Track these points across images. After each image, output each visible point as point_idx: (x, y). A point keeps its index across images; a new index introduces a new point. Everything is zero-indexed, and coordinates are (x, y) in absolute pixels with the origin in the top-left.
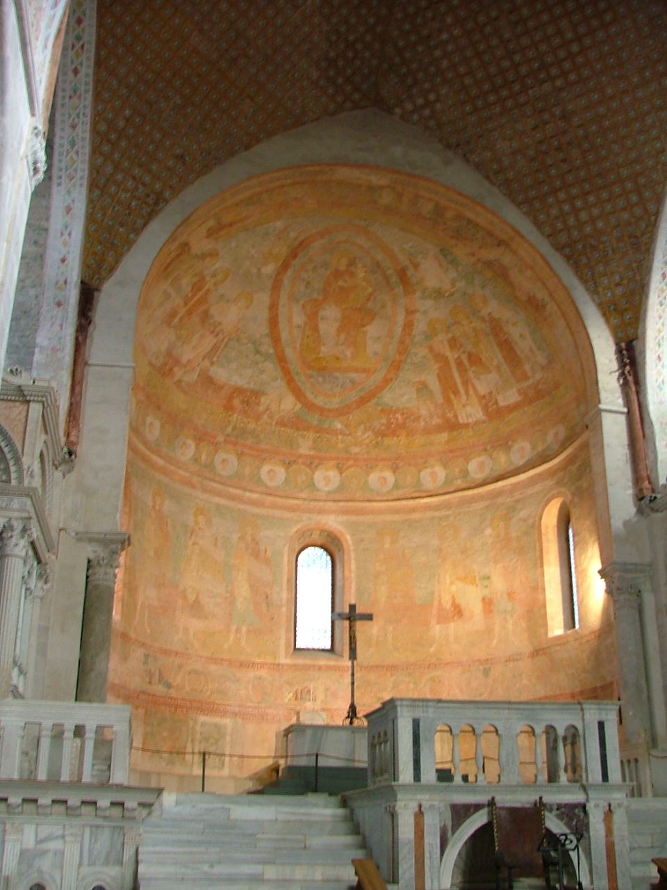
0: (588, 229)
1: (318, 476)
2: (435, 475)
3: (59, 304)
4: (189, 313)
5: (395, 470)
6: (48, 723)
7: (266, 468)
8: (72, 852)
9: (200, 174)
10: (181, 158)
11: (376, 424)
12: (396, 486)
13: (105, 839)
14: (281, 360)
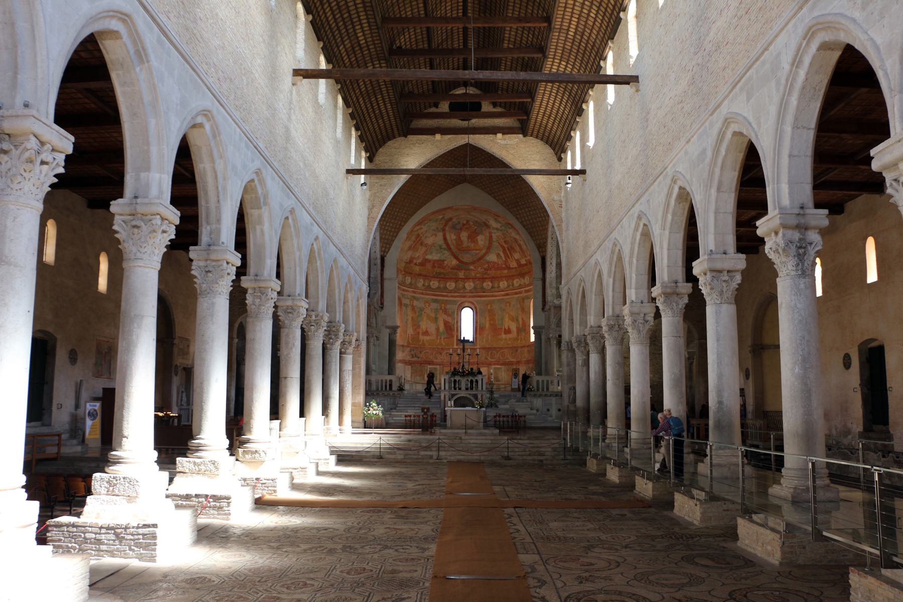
1: (466, 285)
2: (503, 284)
3: (375, 265)
4: (416, 244)
5: (492, 282)
6: (380, 379)
7: (448, 284)
12: (493, 287)
14: (449, 248)
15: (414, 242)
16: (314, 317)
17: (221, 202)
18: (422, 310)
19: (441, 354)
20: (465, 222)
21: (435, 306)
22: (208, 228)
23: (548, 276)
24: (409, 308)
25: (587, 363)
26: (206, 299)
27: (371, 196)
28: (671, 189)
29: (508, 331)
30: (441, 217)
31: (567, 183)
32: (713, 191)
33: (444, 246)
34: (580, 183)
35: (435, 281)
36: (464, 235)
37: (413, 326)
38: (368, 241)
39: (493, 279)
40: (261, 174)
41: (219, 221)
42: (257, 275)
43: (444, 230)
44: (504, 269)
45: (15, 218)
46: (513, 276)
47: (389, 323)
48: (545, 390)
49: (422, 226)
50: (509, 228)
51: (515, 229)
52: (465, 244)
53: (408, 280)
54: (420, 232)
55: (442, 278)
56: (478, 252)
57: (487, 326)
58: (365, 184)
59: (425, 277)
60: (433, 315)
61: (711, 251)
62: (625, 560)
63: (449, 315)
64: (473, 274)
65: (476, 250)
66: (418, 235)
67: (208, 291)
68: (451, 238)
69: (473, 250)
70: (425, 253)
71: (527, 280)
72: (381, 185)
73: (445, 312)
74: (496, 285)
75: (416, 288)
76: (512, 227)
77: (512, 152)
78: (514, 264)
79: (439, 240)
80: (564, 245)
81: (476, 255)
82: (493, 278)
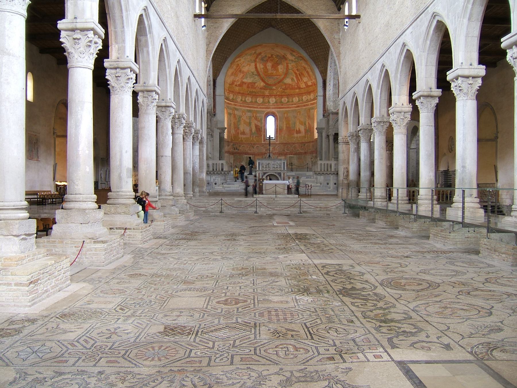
0: (316, 55)
1: (270, 100)
2: (296, 99)
7: (258, 99)
8: (219, 179)
9: (234, 50)
10: (229, 49)
11: (283, 87)
12: (288, 102)
13: (223, 178)
14: (259, 75)
15: (235, 70)
16: (177, 116)
17: (125, 27)
18: (240, 117)
19: (253, 147)
20: (270, 56)
21: (249, 114)
22: (117, 46)
23: (327, 93)
24: (232, 116)
25: (358, 150)
26: (117, 96)
27: (208, 35)
28: (431, 22)
29: (299, 132)
30: (254, 52)
31: (345, 25)
32: (466, 21)
33: (255, 73)
34: (356, 25)
35: (249, 97)
36: (269, 65)
37: (235, 128)
38: (207, 67)
39: (288, 96)
40: (147, 10)
41: (124, 41)
42: (145, 83)
43: (255, 61)
44: (297, 89)
45: (10, 22)
46: (303, 93)
47: (219, 126)
48: (326, 170)
49: (241, 59)
50: (301, 60)
51: (305, 60)
52: (270, 72)
53: (231, 96)
54: (239, 62)
55: (254, 95)
56: (278, 77)
57: (285, 128)
58: (205, 26)
59: (243, 94)
60: (248, 121)
61: (462, 63)
62: (410, 263)
63: (259, 121)
64: (275, 93)
65: (277, 75)
66: (238, 64)
67: (118, 90)
68: (260, 67)
69: (276, 75)
70: (242, 78)
71: (312, 96)
72: (215, 28)
73: (256, 118)
74: (291, 100)
75: (237, 102)
76: (303, 58)
77: (306, 4)
78: (303, 86)
79: (252, 68)
80: (342, 70)
81: (277, 79)
82: (289, 95)
